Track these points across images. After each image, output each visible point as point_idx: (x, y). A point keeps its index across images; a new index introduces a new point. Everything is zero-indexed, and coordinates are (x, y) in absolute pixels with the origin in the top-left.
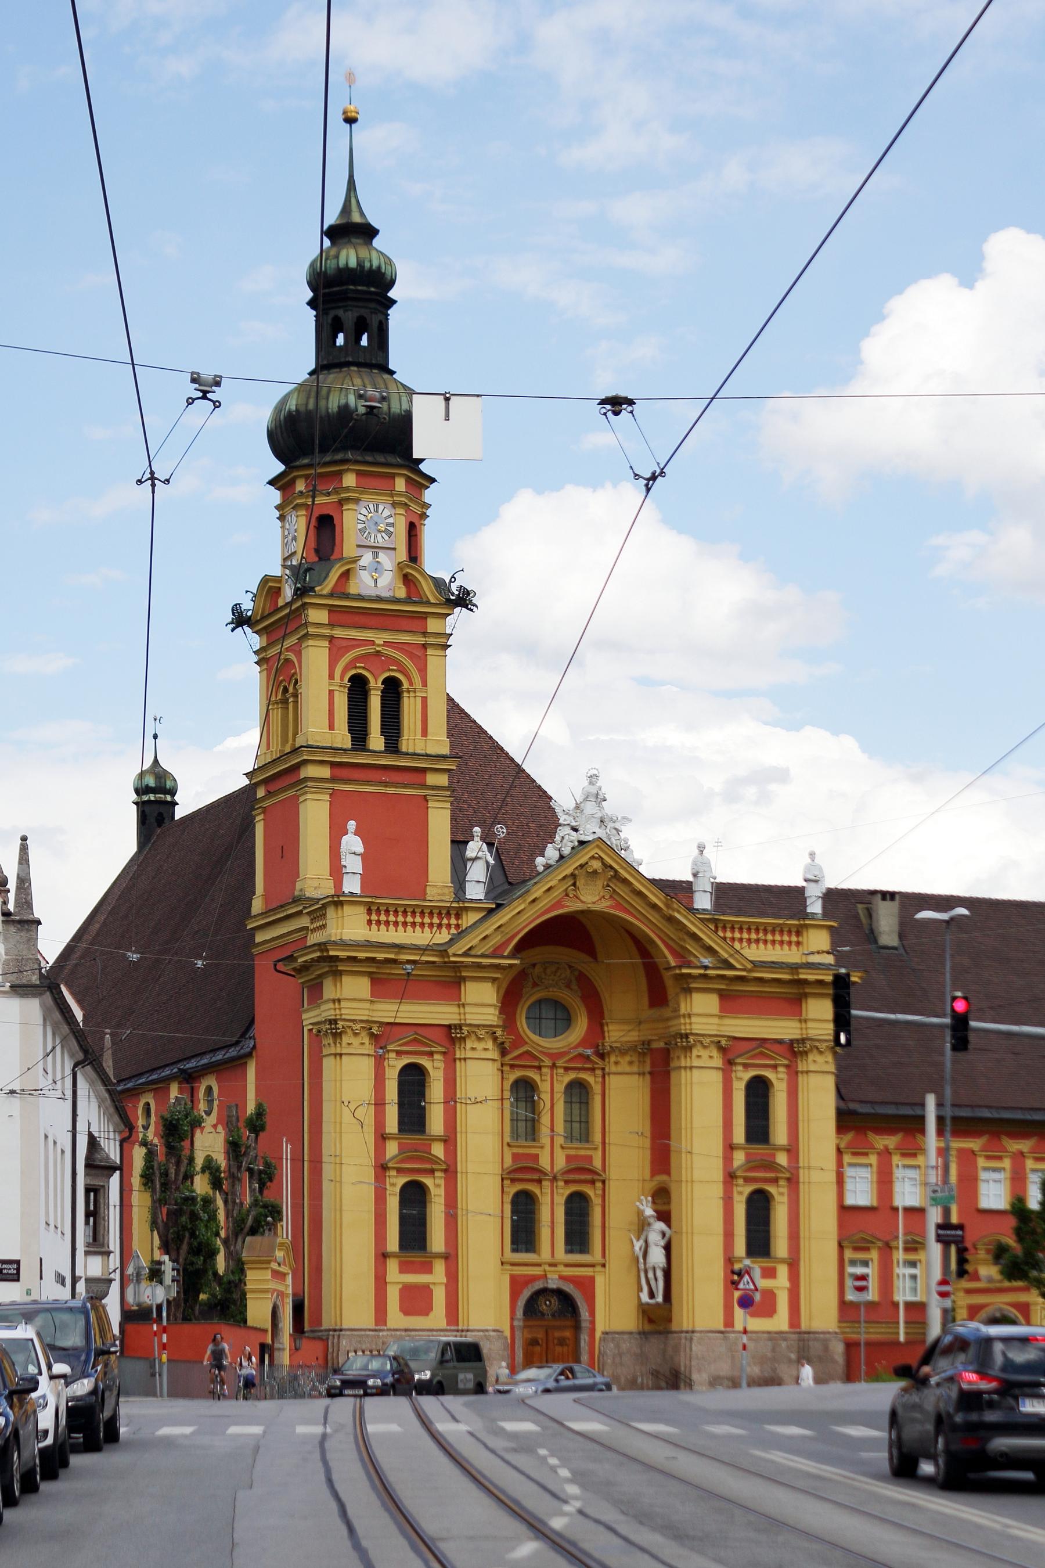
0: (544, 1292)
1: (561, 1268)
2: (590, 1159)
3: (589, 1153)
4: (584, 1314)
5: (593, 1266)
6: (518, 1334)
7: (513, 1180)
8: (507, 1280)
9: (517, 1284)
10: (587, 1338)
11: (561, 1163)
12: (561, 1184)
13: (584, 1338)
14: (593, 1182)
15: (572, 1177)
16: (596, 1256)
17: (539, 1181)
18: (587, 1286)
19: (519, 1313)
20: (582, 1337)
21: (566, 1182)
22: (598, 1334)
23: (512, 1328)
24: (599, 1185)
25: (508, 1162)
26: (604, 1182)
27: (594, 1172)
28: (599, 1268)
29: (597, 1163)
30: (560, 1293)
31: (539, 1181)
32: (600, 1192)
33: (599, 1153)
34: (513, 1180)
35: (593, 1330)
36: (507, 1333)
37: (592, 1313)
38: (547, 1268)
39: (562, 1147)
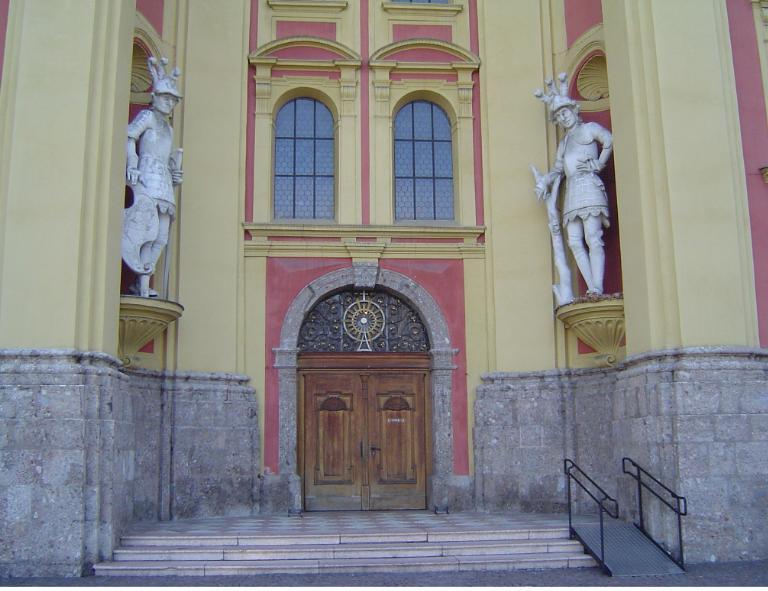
0: (351, 291)
1: (381, 242)
2: (446, 32)
3: (442, 21)
4: (441, 342)
5: (457, 239)
6: (288, 385)
7: (276, 71)
8: (258, 268)
9: (281, 280)
10: (447, 392)
11: (381, 37)
12: (384, 76)
13: (442, 388)
14: (452, 75)
15: (404, 65)
16: (467, 218)
17: (334, 73)
18: (448, 281)
19: (289, 342)
20: (437, 389)
21: (395, 74)
22: (473, 383)
23: (271, 370)
24: (465, 78)
25: (267, 36)
26: (476, 72)
27: (450, 55)
28: (470, 242)
29: (461, 39)
30: (378, 291)
31: (334, 73)
32: (470, 94)
33: (466, 16)
34: (276, 71)
35: (460, 377)
36: (259, 384)
37: (459, 339)
38: (351, 242)
39: (385, 10)
